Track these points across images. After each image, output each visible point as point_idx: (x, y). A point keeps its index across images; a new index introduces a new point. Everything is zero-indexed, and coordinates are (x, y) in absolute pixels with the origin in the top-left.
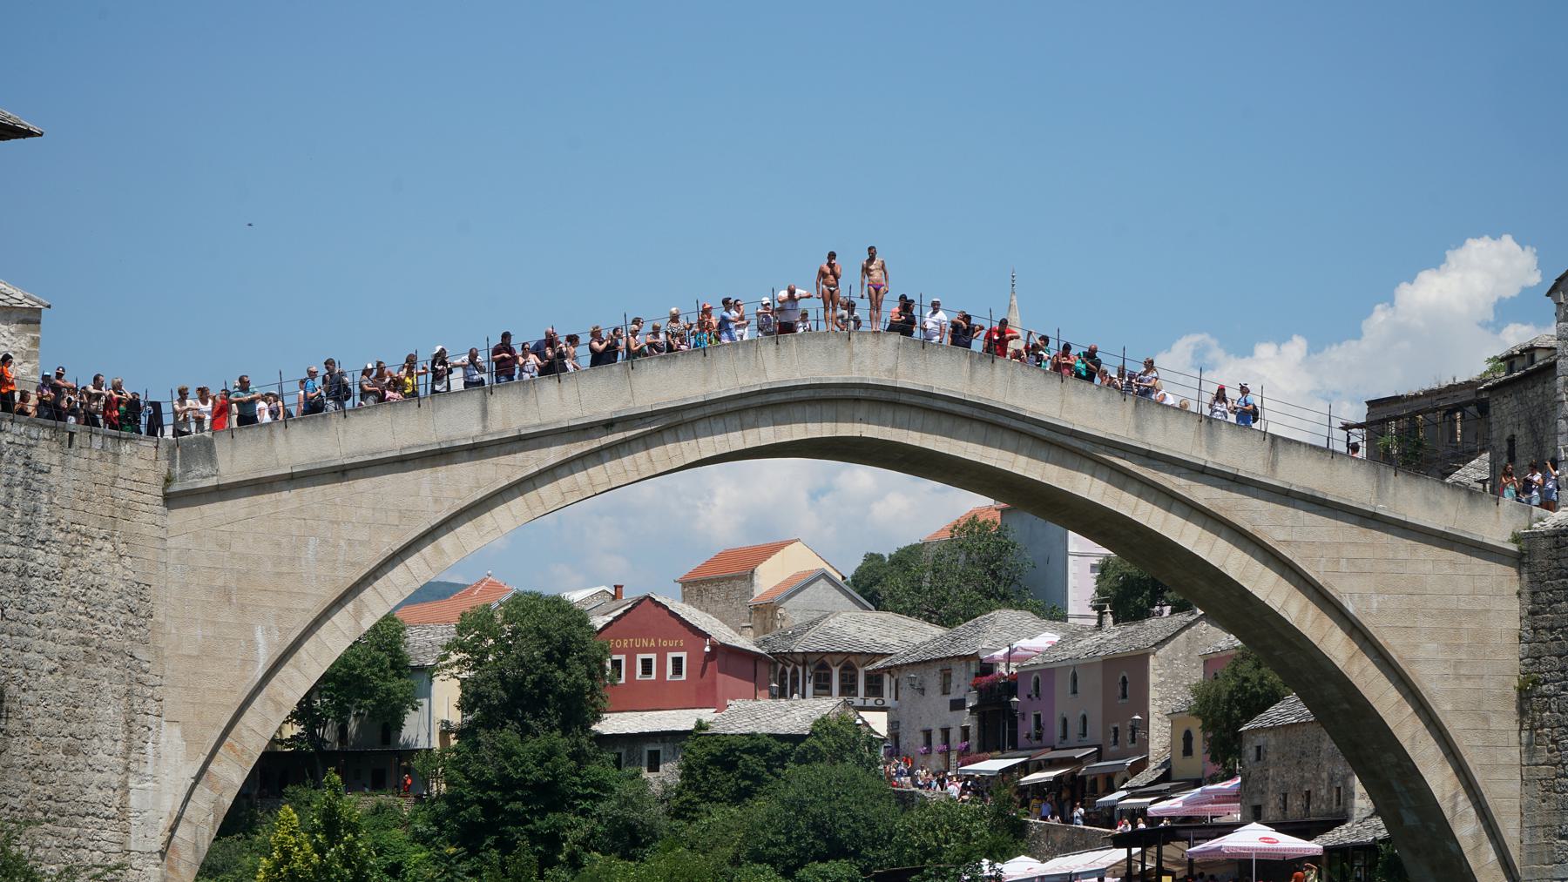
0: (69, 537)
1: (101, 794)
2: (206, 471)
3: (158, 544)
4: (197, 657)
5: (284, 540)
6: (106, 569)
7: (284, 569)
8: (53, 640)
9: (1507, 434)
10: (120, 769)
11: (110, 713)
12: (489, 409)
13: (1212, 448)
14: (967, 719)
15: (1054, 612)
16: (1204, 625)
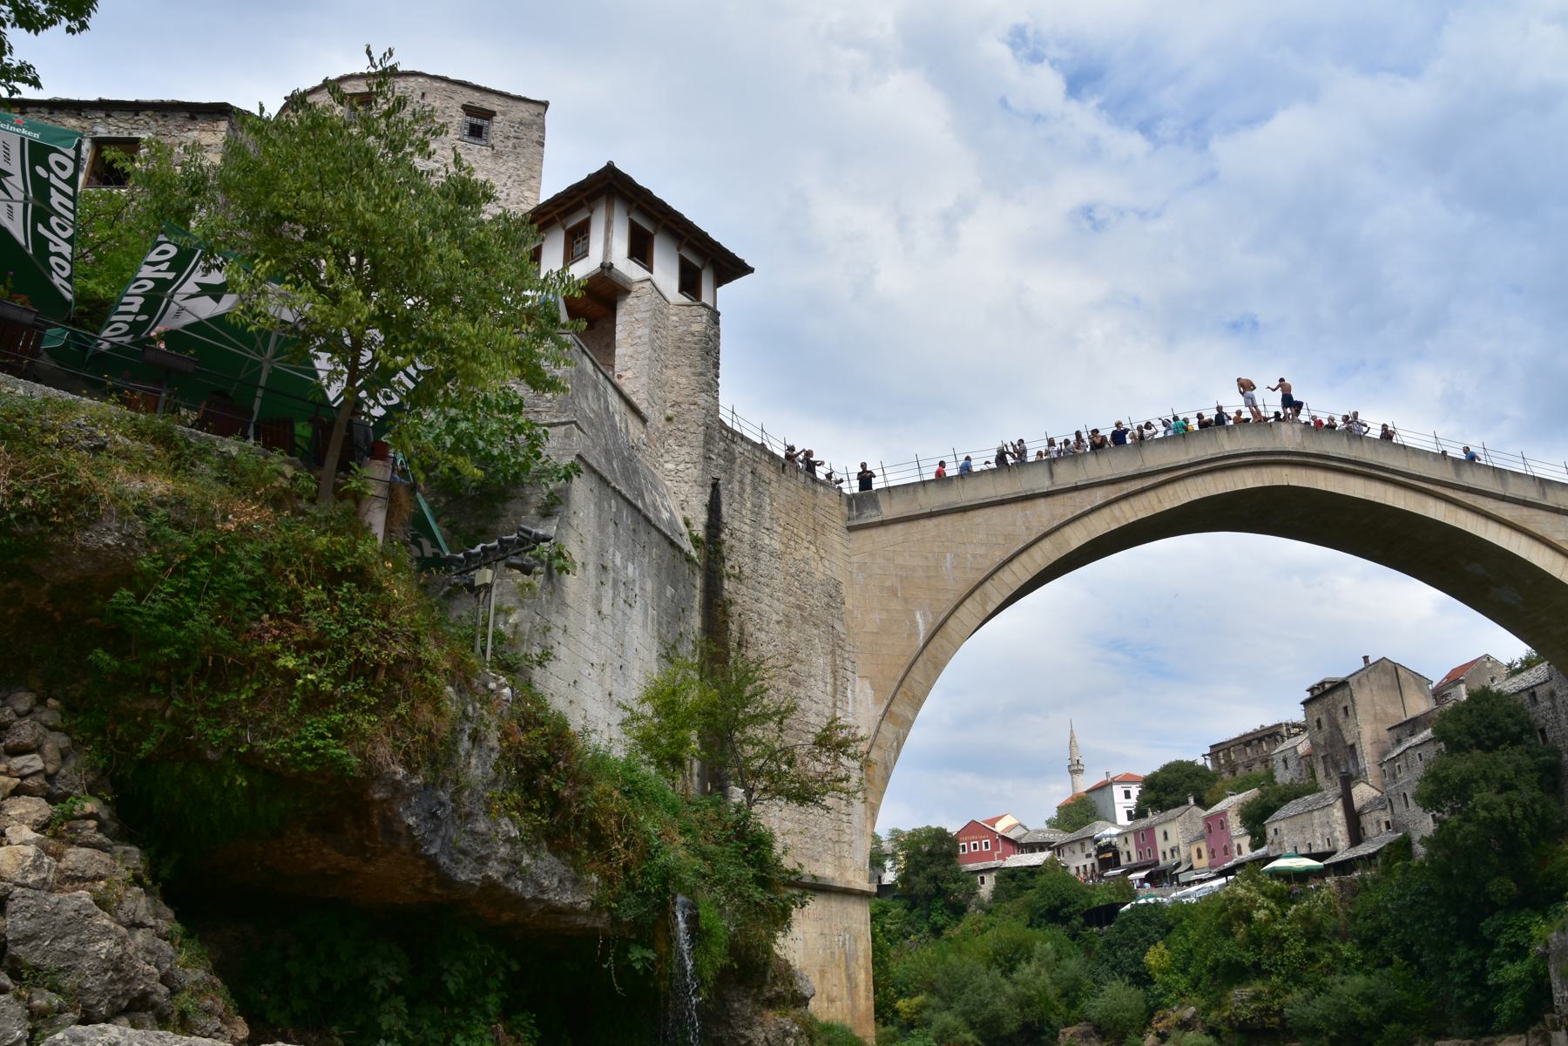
0: (786, 532)
1: (819, 719)
2: (875, 512)
3: (847, 558)
4: (877, 633)
5: (929, 555)
6: (813, 564)
7: (932, 574)
8: (778, 600)
9: (1316, 718)
10: (830, 704)
11: (821, 662)
12: (1054, 472)
13: (1504, 484)
14: (1093, 860)
15: (1114, 822)
16: (1195, 808)
